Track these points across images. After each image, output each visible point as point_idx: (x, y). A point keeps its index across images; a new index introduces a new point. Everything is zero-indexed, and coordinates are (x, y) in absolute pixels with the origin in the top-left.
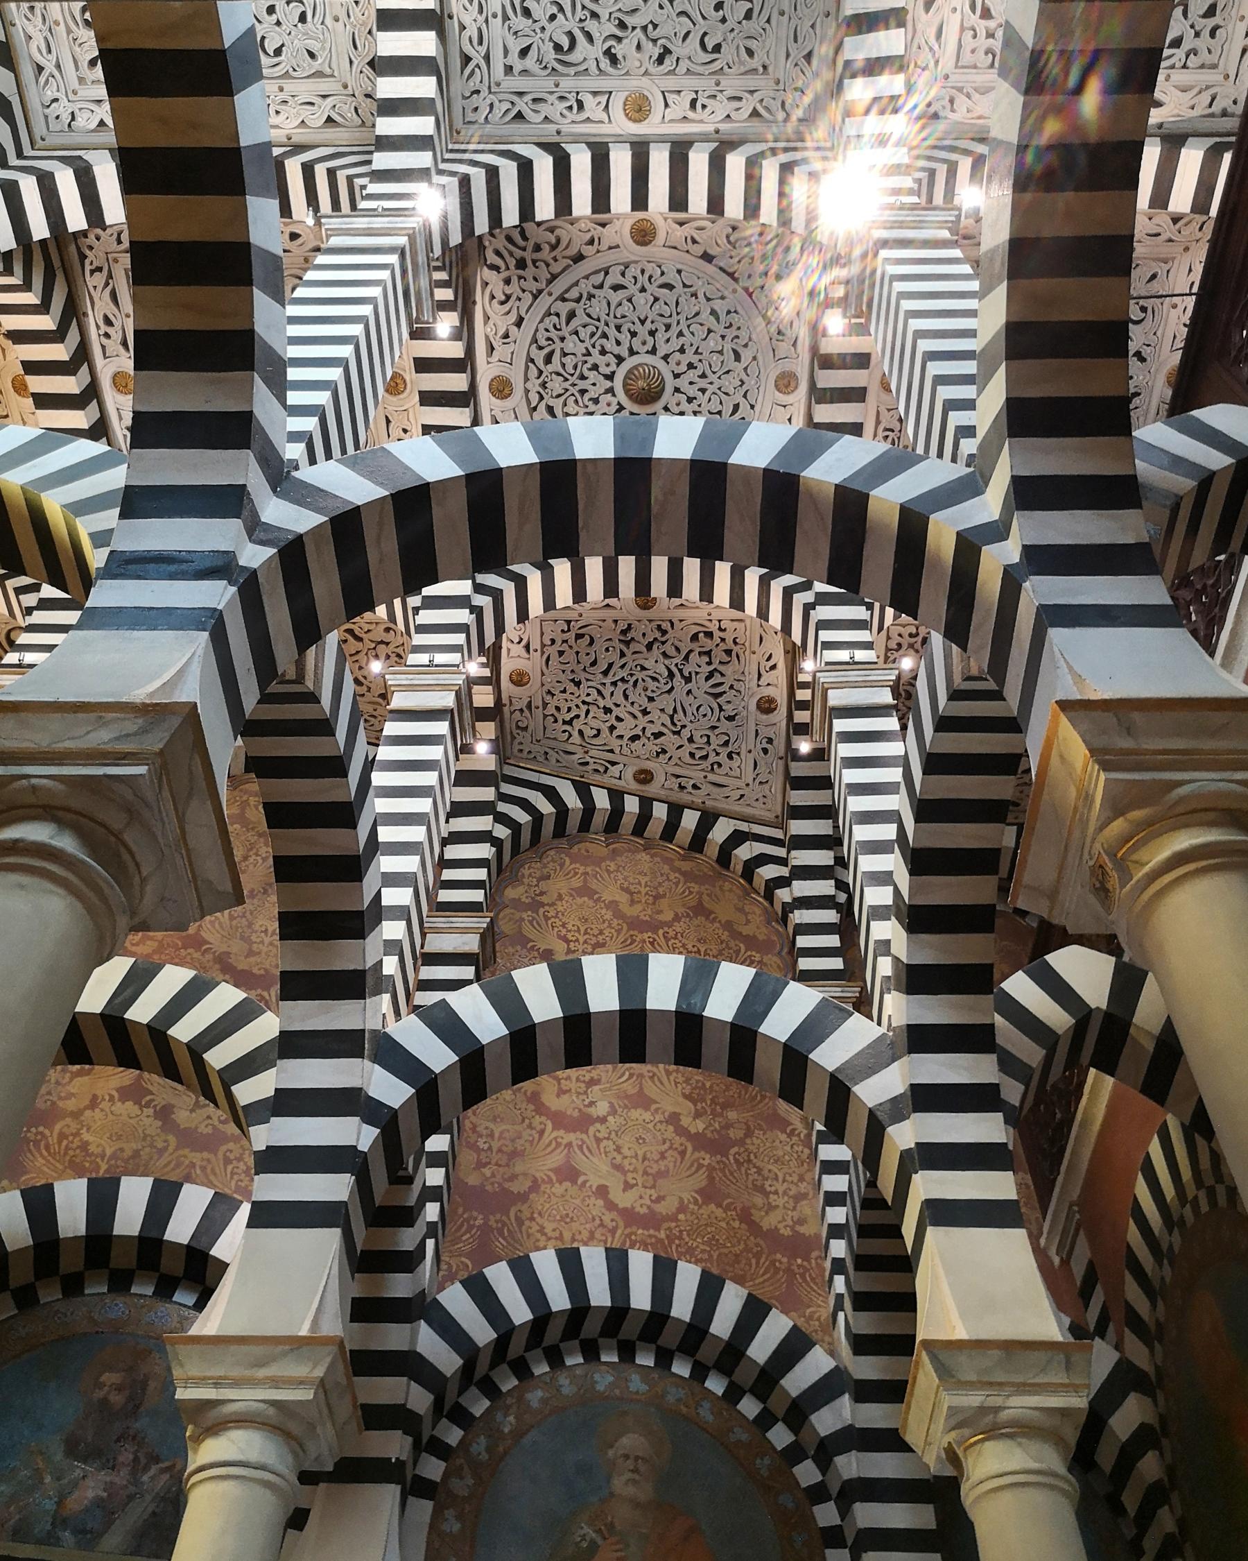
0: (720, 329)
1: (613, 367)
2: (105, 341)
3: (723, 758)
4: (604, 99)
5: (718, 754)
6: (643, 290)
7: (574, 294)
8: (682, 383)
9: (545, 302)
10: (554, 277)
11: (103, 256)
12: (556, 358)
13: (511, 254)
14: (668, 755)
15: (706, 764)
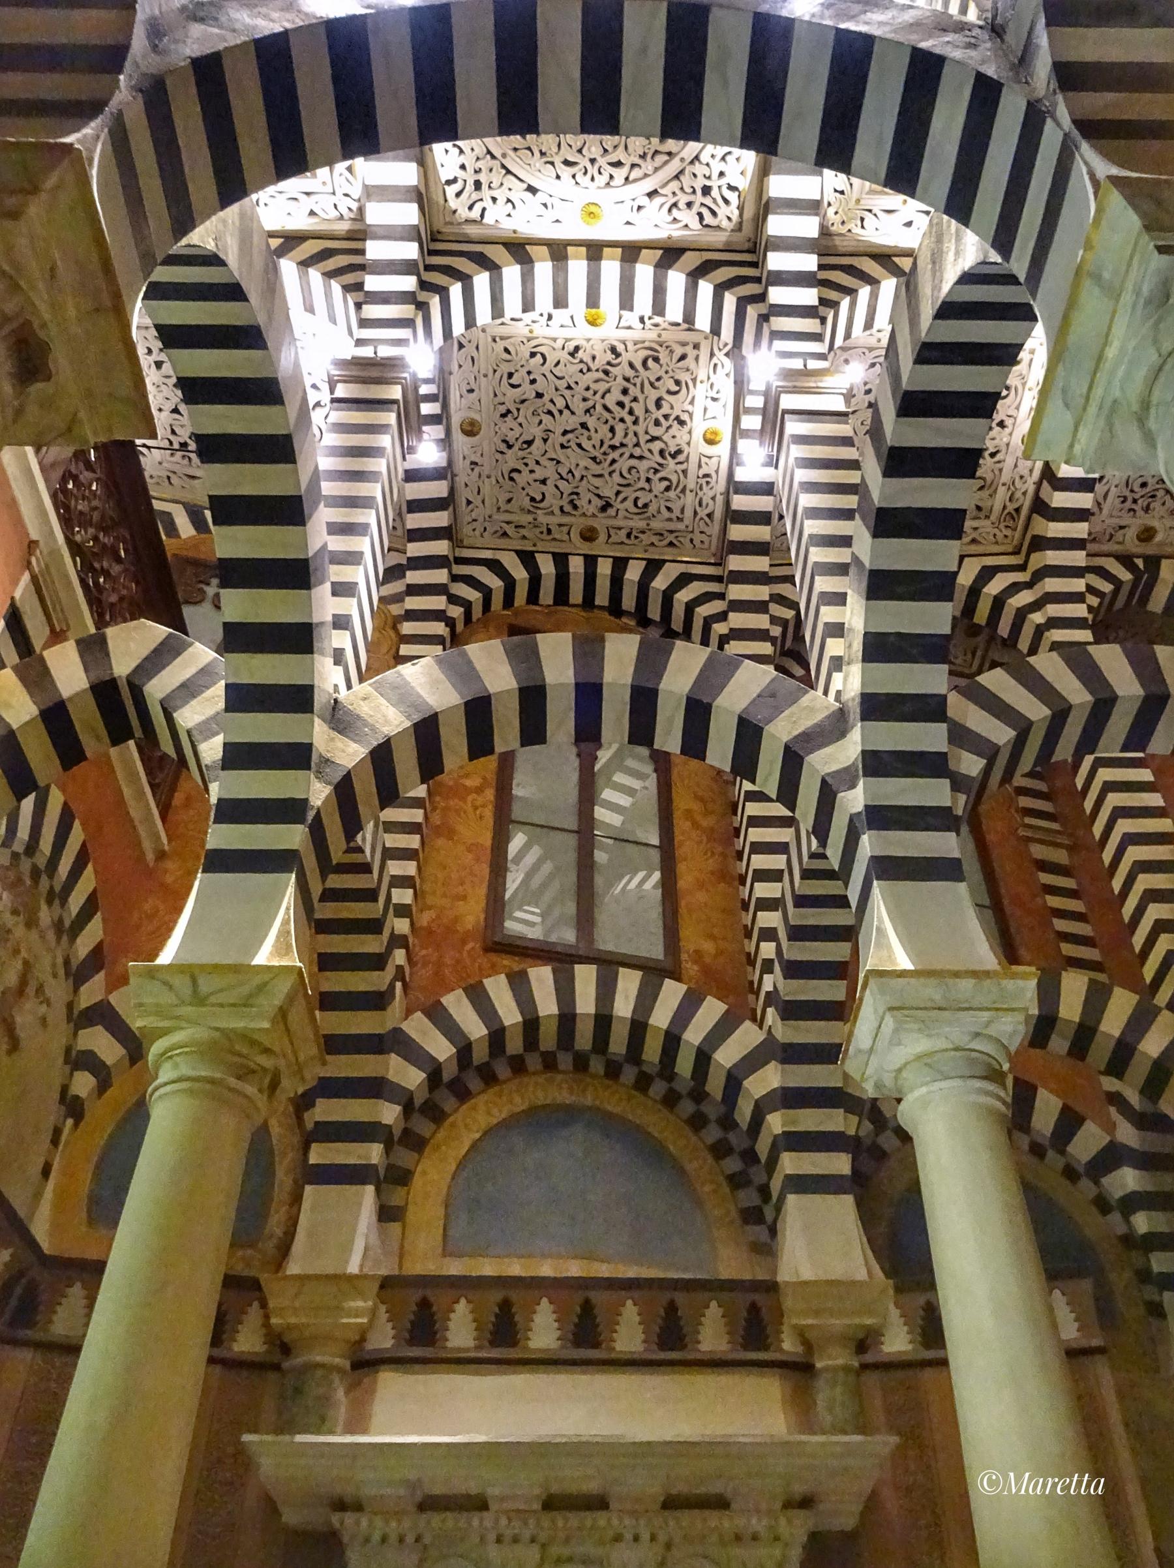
4: (622, 324)
6: (593, 161)
10: (677, 177)
13: (714, 200)
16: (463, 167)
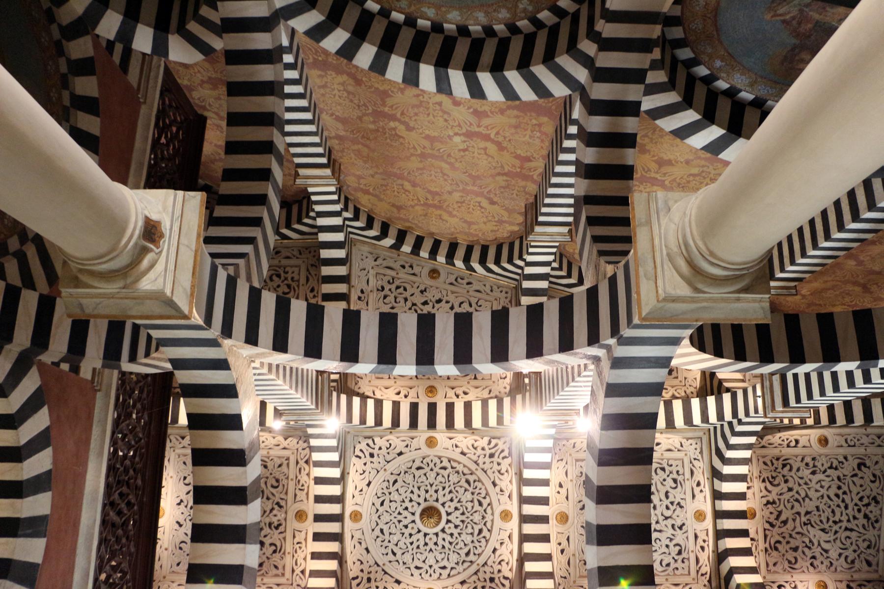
0: (391, 546)
1: (447, 526)
2: (706, 538)
3: (387, 287)
5: (390, 290)
6: (431, 567)
7: (466, 565)
8: (410, 518)
9: (481, 561)
10: (476, 573)
11: (700, 582)
12: (476, 532)
13: (497, 585)
14: (420, 289)
15: (397, 283)
16: (362, 571)
